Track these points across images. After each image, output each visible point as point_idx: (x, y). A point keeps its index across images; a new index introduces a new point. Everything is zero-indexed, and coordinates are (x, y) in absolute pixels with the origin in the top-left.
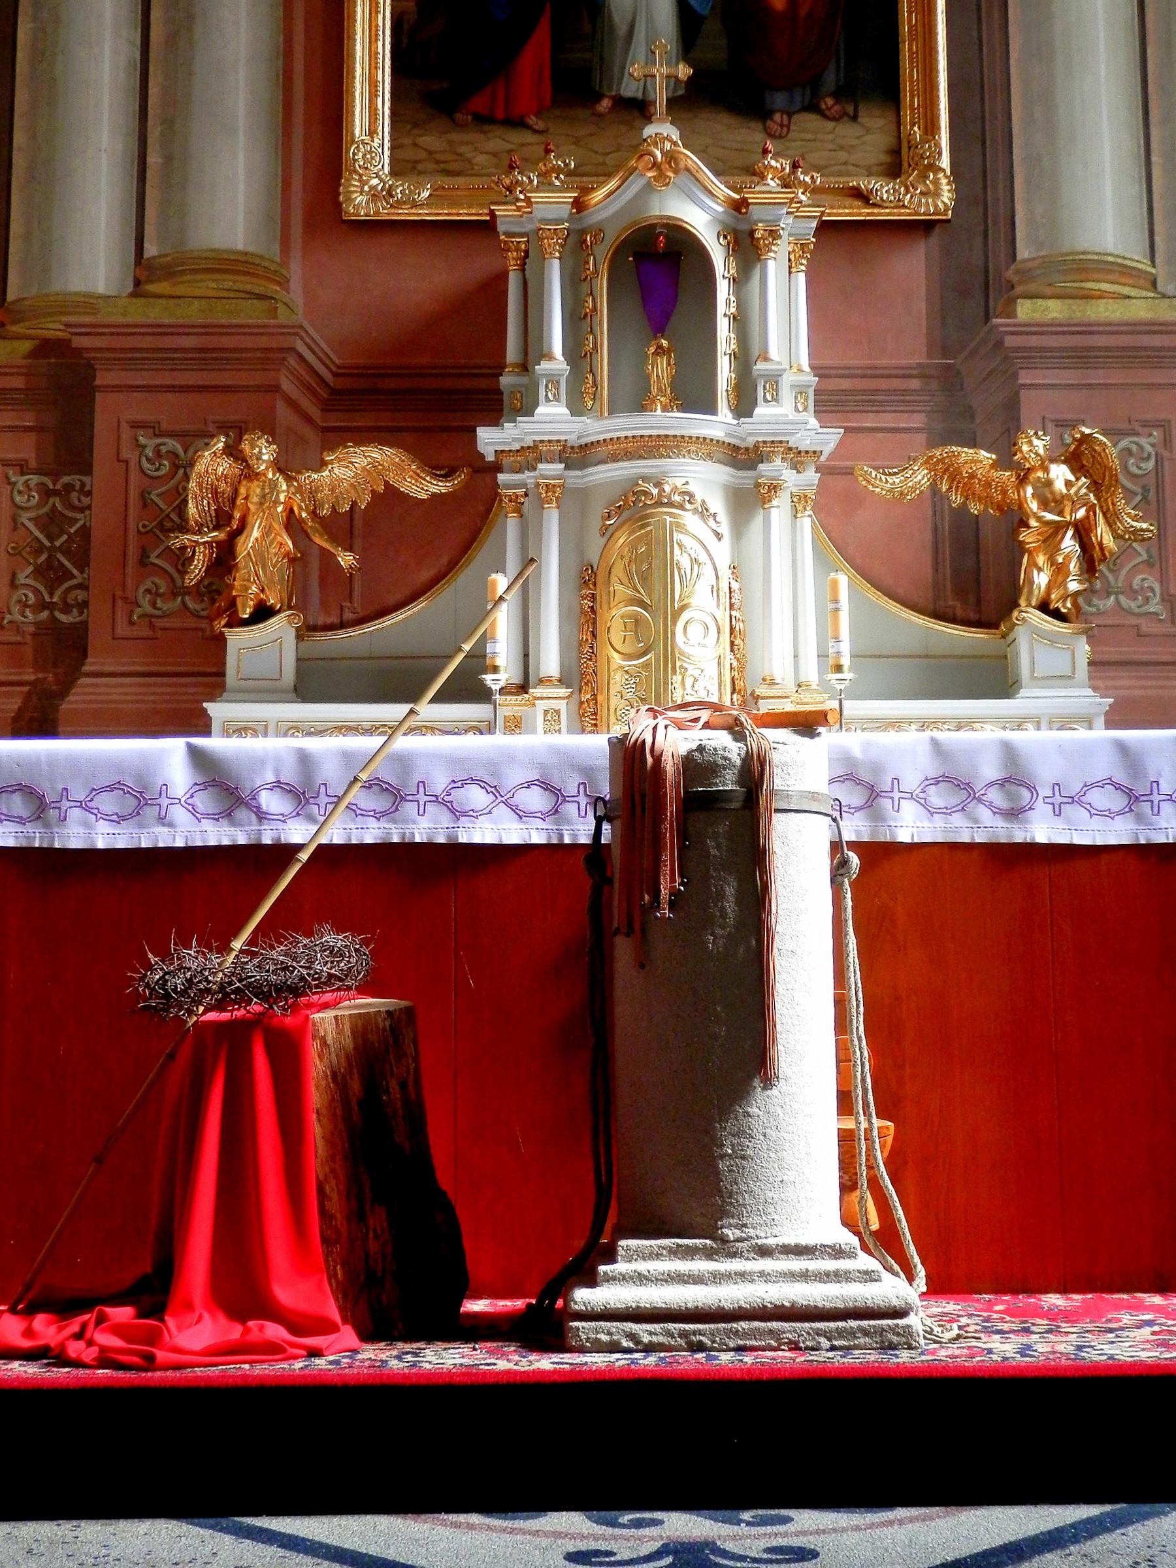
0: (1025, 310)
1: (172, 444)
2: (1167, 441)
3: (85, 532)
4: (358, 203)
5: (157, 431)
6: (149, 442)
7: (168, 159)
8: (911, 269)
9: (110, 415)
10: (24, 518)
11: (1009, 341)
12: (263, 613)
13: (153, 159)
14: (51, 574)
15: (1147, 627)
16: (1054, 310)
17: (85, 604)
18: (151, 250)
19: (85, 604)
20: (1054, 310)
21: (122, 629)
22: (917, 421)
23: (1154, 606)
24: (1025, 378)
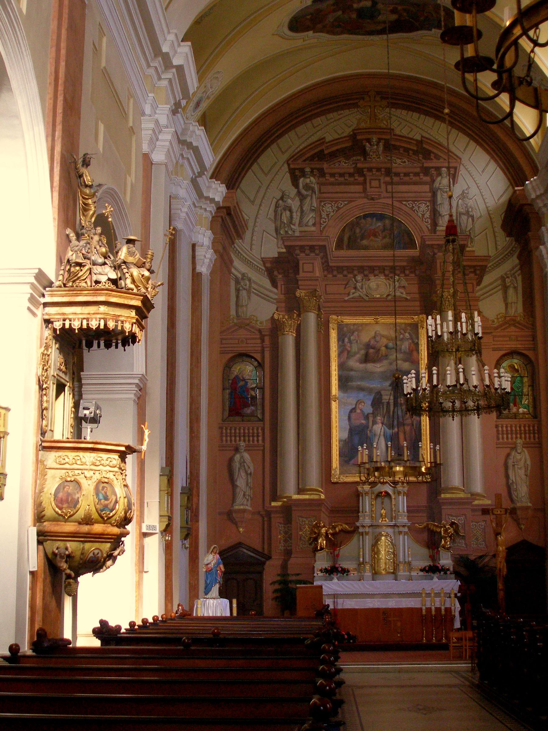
0: (443, 496)
1: (305, 519)
2: (466, 518)
3: (291, 534)
4: (334, 480)
5: (301, 517)
6: (301, 519)
7: (303, 472)
8: (424, 489)
9: (295, 515)
10: (281, 532)
11: (440, 501)
12: (322, 549)
13: (300, 471)
14: (286, 541)
15: (462, 548)
16: (448, 496)
17: (291, 546)
18: (300, 487)
19: (291, 546)
20: (448, 496)
21: (298, 550)
22: (425, 515)
23: (463, 545)
24: (443, 507)
